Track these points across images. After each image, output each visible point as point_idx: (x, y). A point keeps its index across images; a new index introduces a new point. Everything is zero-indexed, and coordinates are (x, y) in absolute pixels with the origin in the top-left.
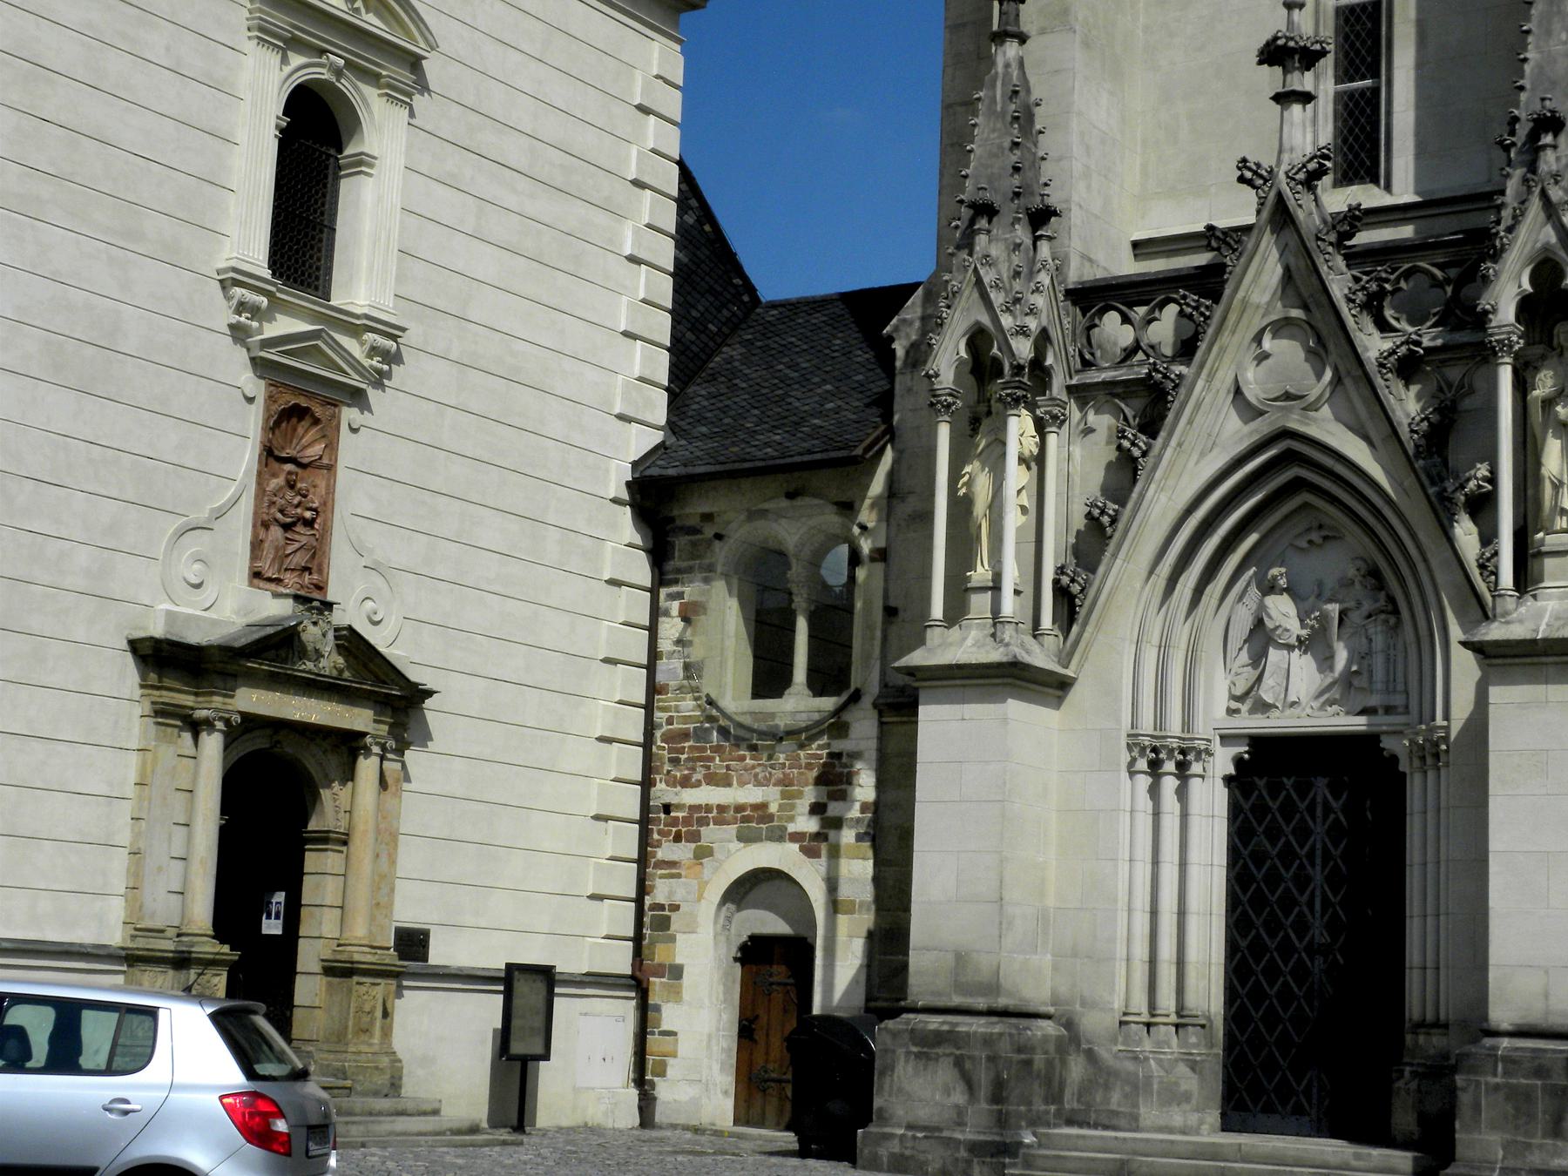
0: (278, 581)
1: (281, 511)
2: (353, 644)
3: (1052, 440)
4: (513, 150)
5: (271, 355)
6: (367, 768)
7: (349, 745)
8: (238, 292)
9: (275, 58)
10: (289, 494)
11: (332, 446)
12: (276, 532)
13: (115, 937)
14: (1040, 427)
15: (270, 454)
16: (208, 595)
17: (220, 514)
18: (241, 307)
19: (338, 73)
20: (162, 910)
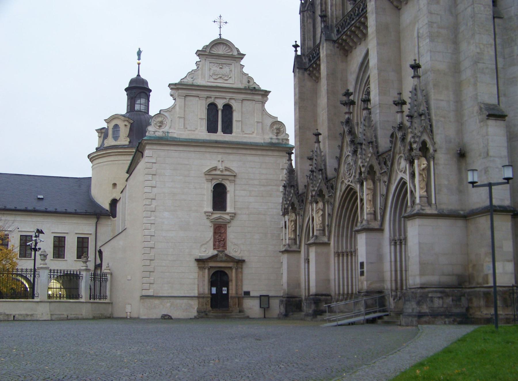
0: (218, 249)
1: (218, 240)
2: (227, 255)
3: (298, 217)
4: (256, 182)
5: (212, 221)
6: (234, 271)
7: (230, 268)
8: (206, 214)
9: (210, 183)
10: (219, 237)
11: (226, 230)
12: (217, 243)
13: (197, 295)
14: (296, 216)
15: (215, 233)
16: (207, 252)
17: (208, 242)
18: (207, 216)
19: (221, 181)
20: (201, 291)
